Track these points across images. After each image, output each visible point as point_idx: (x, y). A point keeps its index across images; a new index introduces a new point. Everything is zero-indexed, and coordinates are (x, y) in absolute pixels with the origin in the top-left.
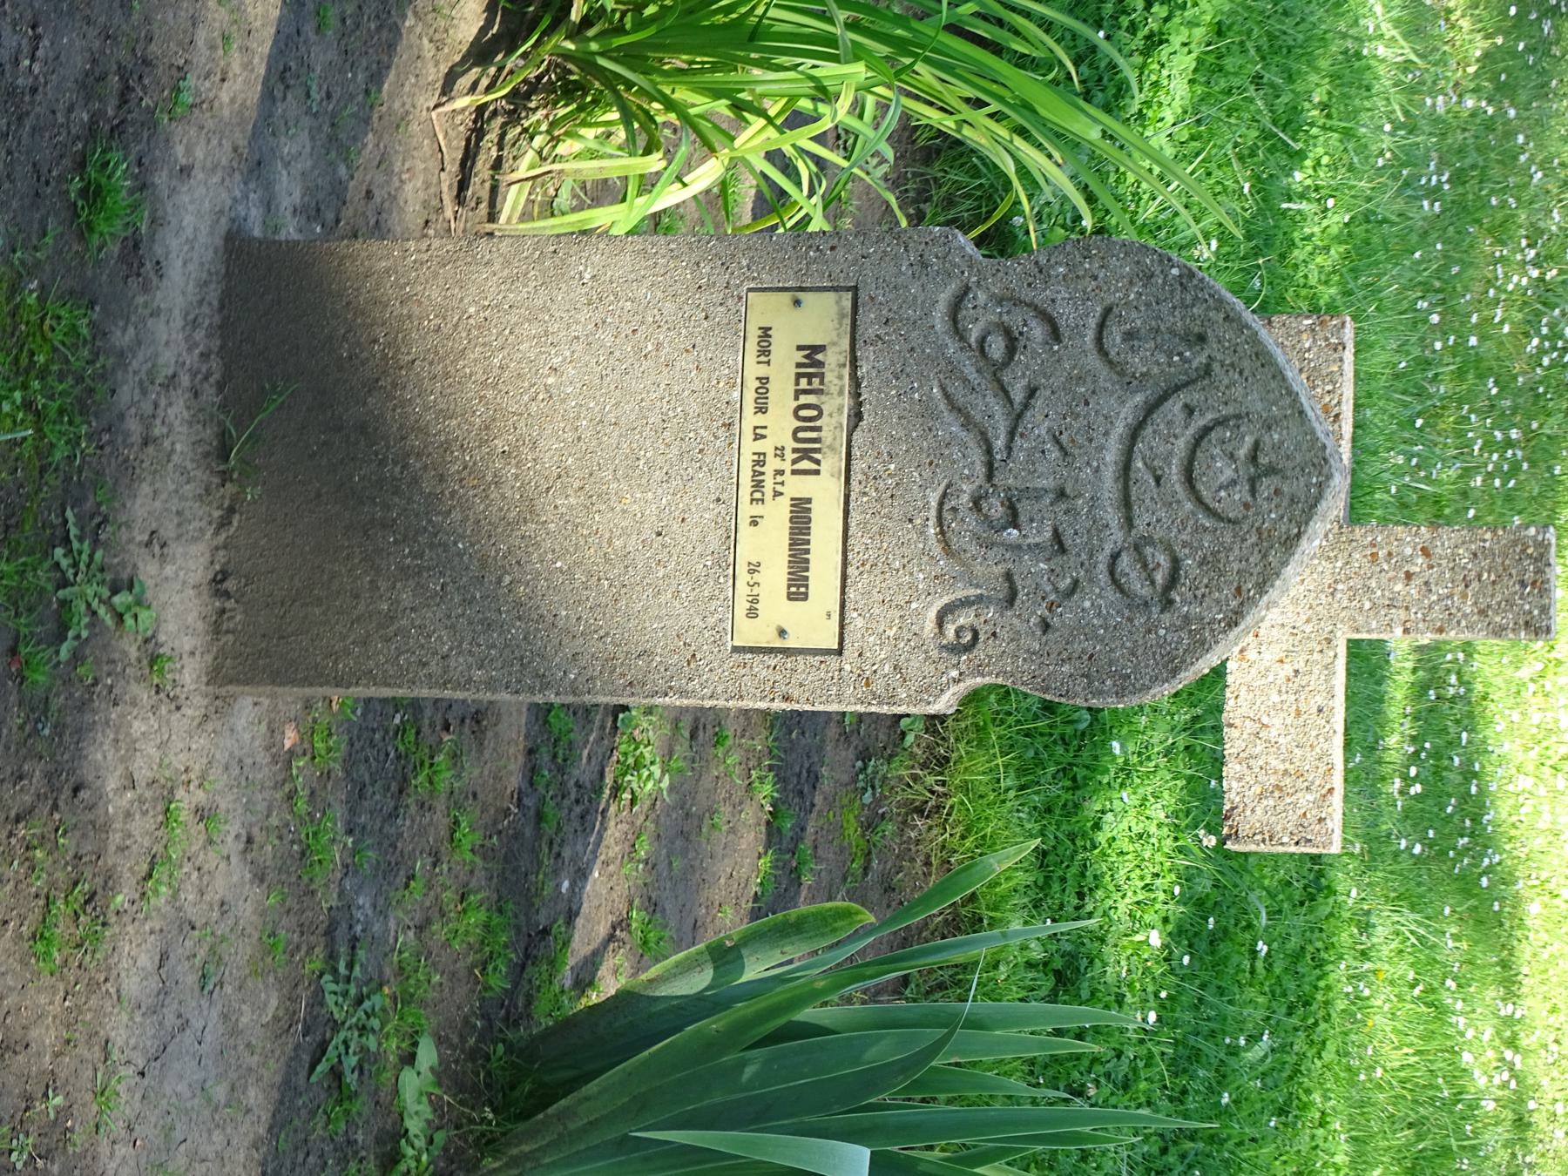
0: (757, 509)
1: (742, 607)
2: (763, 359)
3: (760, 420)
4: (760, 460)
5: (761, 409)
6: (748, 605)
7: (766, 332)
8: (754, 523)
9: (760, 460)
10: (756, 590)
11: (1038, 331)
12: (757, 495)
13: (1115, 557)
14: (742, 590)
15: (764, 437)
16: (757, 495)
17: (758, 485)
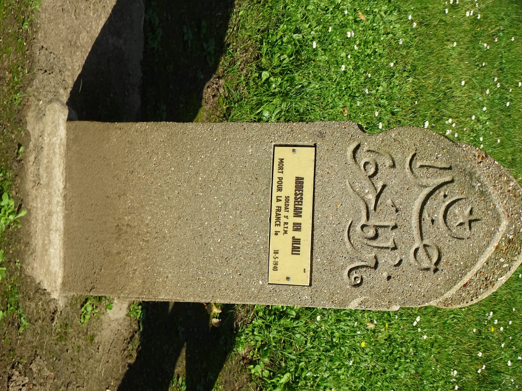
0: (278, 229)
1: (271, 266)
2: (280, 171)
3: (279, 194)
4: (279, 209)
5: (280, 189)
6: (274, 266)
7: (282, 160)
8: (276, 234)
9: (279, 209)
10: (276, 261)
11: (388, 163)
12: (278, 223)
13: (416, 250)
14: (272, 260)
15: (281, 200)
16: (278, 223)
17: (278, 219)
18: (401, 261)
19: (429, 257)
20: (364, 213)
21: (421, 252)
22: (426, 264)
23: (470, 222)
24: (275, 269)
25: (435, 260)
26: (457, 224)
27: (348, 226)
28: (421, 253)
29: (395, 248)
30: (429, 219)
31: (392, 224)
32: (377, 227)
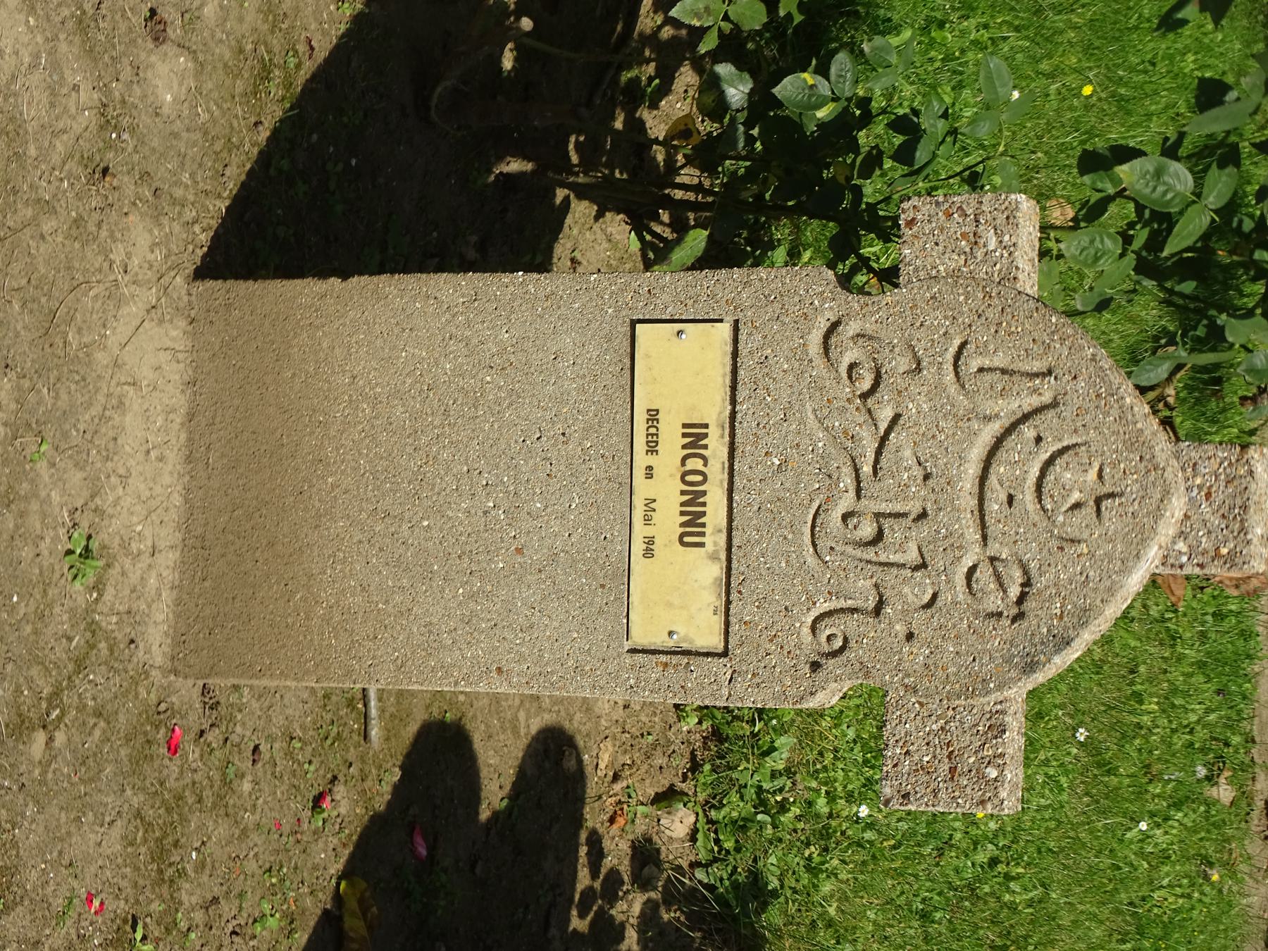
11: (904, 363)
18: (935, 596)
19: (1002, 587)
20: (848, 481)
21: (984, 575)
22: (993, 602)
23: (1098, 501)
24: (649, 553)
25: (1014, 591)
26: (1068, 505)
27: (811, 517)
28: (984, 575)
29: (924, 565)
30: (1003, 497)
31: (914, 508)
32: (878, 516)
